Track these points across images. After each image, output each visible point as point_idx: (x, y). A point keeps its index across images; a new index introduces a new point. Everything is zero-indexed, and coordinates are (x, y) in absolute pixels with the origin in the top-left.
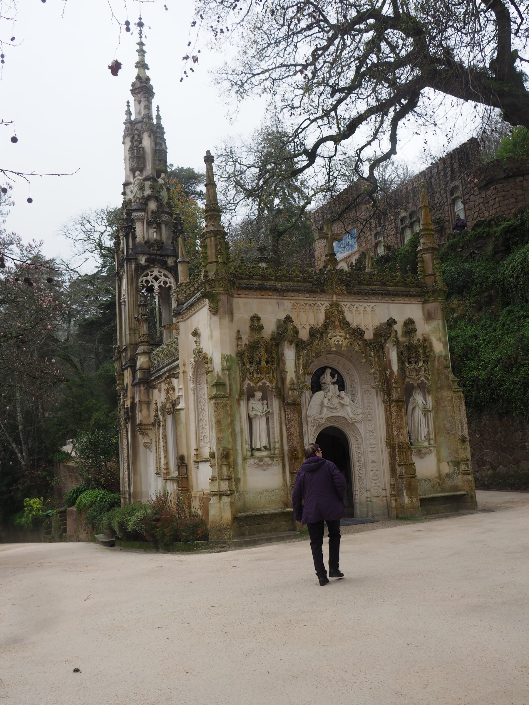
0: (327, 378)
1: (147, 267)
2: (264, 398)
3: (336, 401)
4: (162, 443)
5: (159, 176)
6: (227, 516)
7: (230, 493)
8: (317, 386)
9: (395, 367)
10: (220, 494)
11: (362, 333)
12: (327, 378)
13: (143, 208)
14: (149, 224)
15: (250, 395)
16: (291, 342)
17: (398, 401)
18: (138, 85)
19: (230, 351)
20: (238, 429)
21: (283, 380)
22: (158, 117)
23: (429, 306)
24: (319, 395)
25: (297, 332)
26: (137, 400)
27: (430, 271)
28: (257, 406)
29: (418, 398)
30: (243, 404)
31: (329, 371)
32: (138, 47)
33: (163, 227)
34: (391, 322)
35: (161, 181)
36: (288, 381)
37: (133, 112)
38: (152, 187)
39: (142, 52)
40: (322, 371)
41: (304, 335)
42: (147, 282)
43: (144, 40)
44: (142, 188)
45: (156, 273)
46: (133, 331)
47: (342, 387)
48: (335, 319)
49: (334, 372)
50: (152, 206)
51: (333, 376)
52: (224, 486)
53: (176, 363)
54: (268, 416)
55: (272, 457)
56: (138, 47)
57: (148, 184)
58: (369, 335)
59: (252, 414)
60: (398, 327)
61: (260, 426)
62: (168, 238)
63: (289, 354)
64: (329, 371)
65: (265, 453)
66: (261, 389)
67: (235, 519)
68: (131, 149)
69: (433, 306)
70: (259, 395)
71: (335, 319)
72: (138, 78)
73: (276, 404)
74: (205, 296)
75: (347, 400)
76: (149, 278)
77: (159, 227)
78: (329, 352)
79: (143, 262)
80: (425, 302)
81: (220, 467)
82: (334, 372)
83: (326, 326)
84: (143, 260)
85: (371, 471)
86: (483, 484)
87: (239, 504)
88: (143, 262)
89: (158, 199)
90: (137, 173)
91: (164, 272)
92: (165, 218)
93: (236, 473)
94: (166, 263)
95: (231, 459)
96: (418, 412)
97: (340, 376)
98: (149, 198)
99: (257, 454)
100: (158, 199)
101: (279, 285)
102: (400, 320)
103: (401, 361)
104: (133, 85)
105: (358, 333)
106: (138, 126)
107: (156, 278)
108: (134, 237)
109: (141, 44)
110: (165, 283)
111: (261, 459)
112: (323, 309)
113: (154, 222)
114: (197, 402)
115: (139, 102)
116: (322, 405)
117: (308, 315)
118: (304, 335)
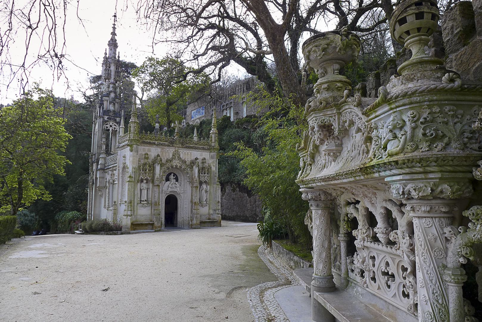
0: (172, 177)
1: (107, 121)
2: (146, 183)
3: (174, 185)
4: (107, 195)
5: (116, 82)
6: (129, 223)
7: (131, 215)
8: (167, 179)
9: (197, 175)
10: (127, 216)
11: (185, 162)
13: (108, 95)
14: (110, 103)
15: (142, 181)
16: (158, 164)
17: (197, 187)
18: (111, 42)
19: (136, 166)
20: (136, 193)
22: (119, 57)
23: (212, 154)
25: (161, 160)
26: (98, 176)
27: (213, 141)
28: (144, 185)
30: (139, 184)
31: (173, 174)
32: (113, 26)
33: (116, 104)
35: (117, 85)
36: (156, 177)
37: (108, 53)
38: (113, 87)
39: (114, 28)
40: (170, 174)
41: (164, 161)
42: (107, 127)
43: (116, 23)
44: (109, 87)
45: (111, 124)
46: (100, 147)
47: (177, 180)
48: (176, 155)
49: (174, 175)
50: (112, 95)
51: (174, 176)
52: (129, 213)
53: (115, 165)
54: (148, 189)
56: (113, 26)
57: (111, 86)
60: (199, 161)
61: (144, 192)
62: (118, 109)
63: (158, 168)
64: (173, 174)
65: (145, 202)
66: (145, 179)
67: (132, 224)
68: (106, 70)
69: (214, 154)
70: (145, 181)
71: (176, 155)
72: (112, 39)
73: (151, 185)
74: (128, 145)
76: (108, 126)
77: (114, 104)
79: (106, 119)
80: (211, 152)
81: (128, 206)
82: (174, 175)
83: (172, 158)
84: (106, 118)
85: (184, 212)
86: (224, 218)
87: (134, 220)
88: (106, 119)
89: (115, 93)
90: (107, 80)
91: (114, 124)
92: (117, 100)
93: (134, 208)
94: (116, 120)
95: (132, 204)
97: (176, 176)
98: (111, 92)
99: (142, 202)
100: (115, 93)
101: (156, 142)
104: (109, 42)
106: (109, 60)
107: (111, 126)
108: (103, 108)
109: (114, 25)
110: (115, 128)
111: (143, 204)
113: (113, 102)
114: (123, 181)
115: (111, 50)
116: (168, 186)
117: (168, 153)
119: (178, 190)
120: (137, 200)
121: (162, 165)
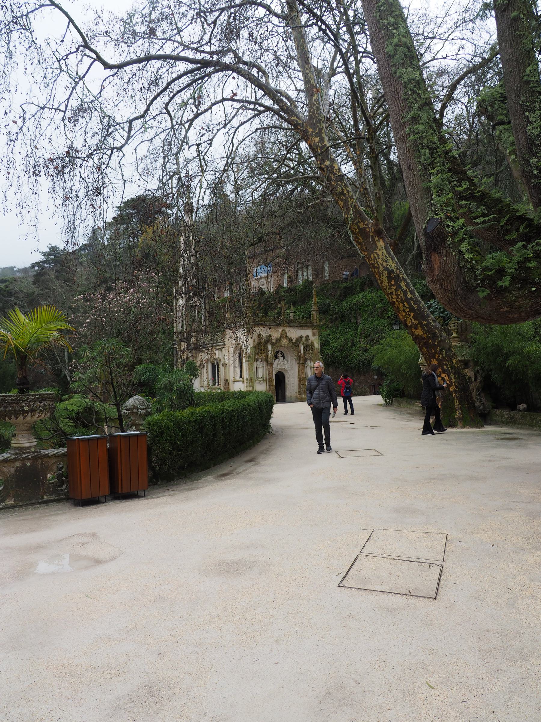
0: (280, 355)
3: (282, 363)
11: (292, 340)
12: (280, 355)
15: (257, 360)
17: (302, 364)
21: (268, 356)
23: (314, 331)
24: (277, 360)
27: (315, 318)
28: (259, 364)
29: (309, 362)
34: (302, 337)
40: (278, 352)
41: (274, 341)
48: (284, 335)
49: (282, 353)
55: (263, 380)
58: (294, 341)
59: (258, 366)
60: (304, 339)
61: (260, 371)
63: (270, 347)
66: (261, 359)
70: (260, 360)
71: (284, 335)
73: (265, 363)
75: (286, 362)
78: (281, 346)
80: (313, 329)
82: (282, 353)
83: (281, 338)
96: (308, 368)
102: (304, 336)
103: (304, 350)
105: (290, 340)
111: (260, 381)
112: (280, 331)
116: (278, 364)
118: (274, 341)
119: (286, 367)
120: (255, 378)
121: (273, 344)
